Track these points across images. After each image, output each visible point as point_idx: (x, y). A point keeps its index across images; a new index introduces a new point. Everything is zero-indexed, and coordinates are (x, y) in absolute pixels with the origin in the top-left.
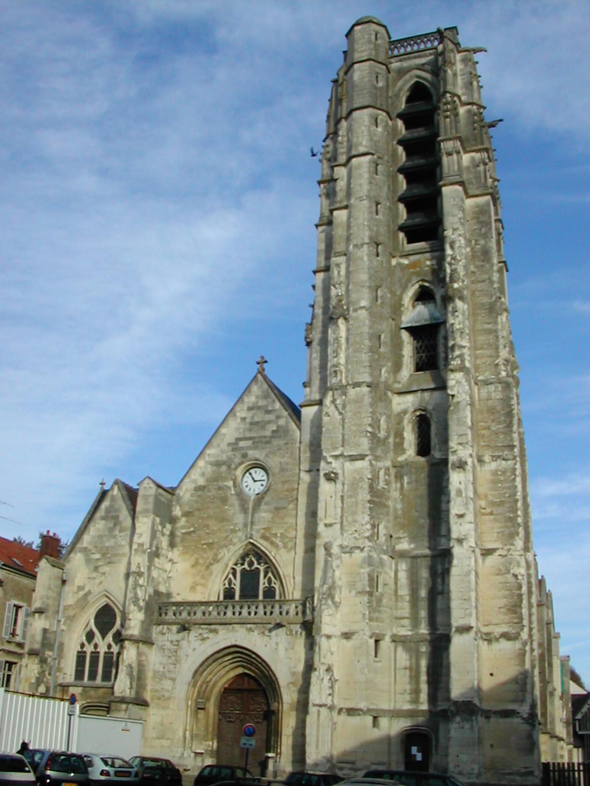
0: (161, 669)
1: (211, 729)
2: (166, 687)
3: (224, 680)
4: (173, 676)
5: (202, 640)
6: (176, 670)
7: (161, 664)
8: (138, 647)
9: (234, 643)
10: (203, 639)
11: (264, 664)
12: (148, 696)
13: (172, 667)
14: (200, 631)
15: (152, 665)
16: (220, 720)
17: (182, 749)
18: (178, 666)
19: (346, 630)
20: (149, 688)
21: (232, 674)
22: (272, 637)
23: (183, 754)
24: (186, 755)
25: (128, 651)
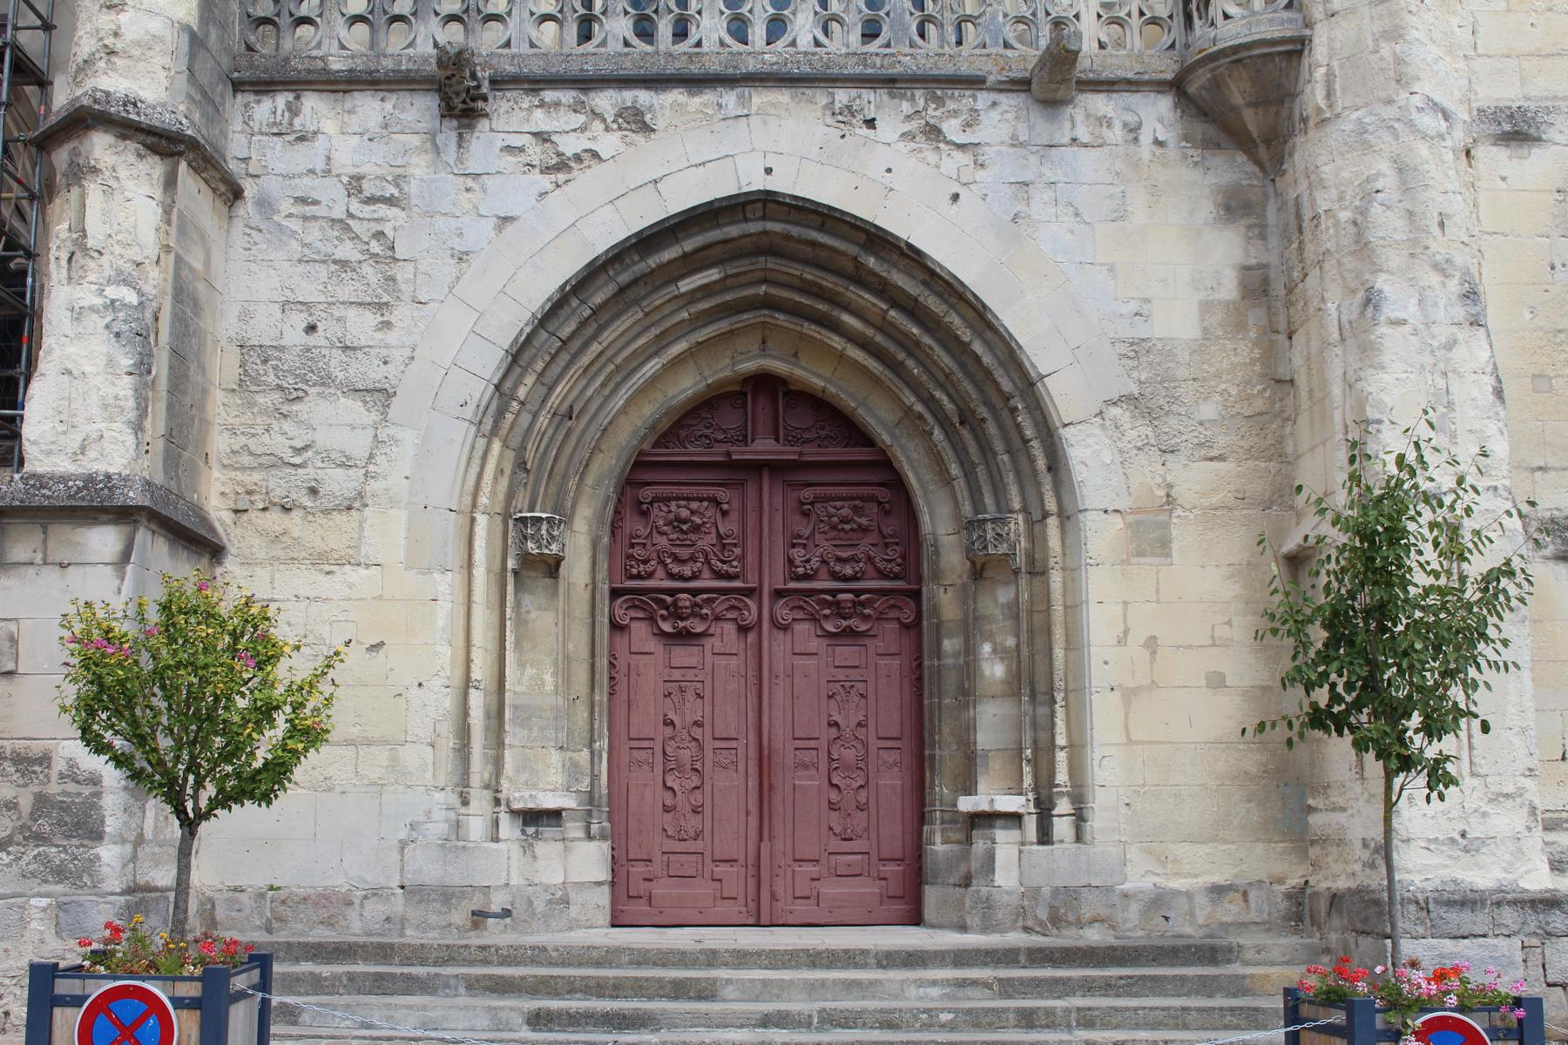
0: (294, 336)
1: (581, 674)
2: (323, 438)
3: (648, 411)
4: (375, 374)
5: (547, 170)
6: (391, 337)
7: (285, 306)
8: (170, 183)
9: (758, 183)
10: (562, 165)
11: (933, 303)
12: (214, 498)
13: (361, 325)
14: (541, 120)
15: (233, 312)
16: (616, 627)
17: (454, 799)
18: (402, 314)
19: (1503, 91)
20: (219, 443)
21: (687, 385)
22: (989, 154)
23: (457, 826)
24: (476, 827)
25: (108, 191)
